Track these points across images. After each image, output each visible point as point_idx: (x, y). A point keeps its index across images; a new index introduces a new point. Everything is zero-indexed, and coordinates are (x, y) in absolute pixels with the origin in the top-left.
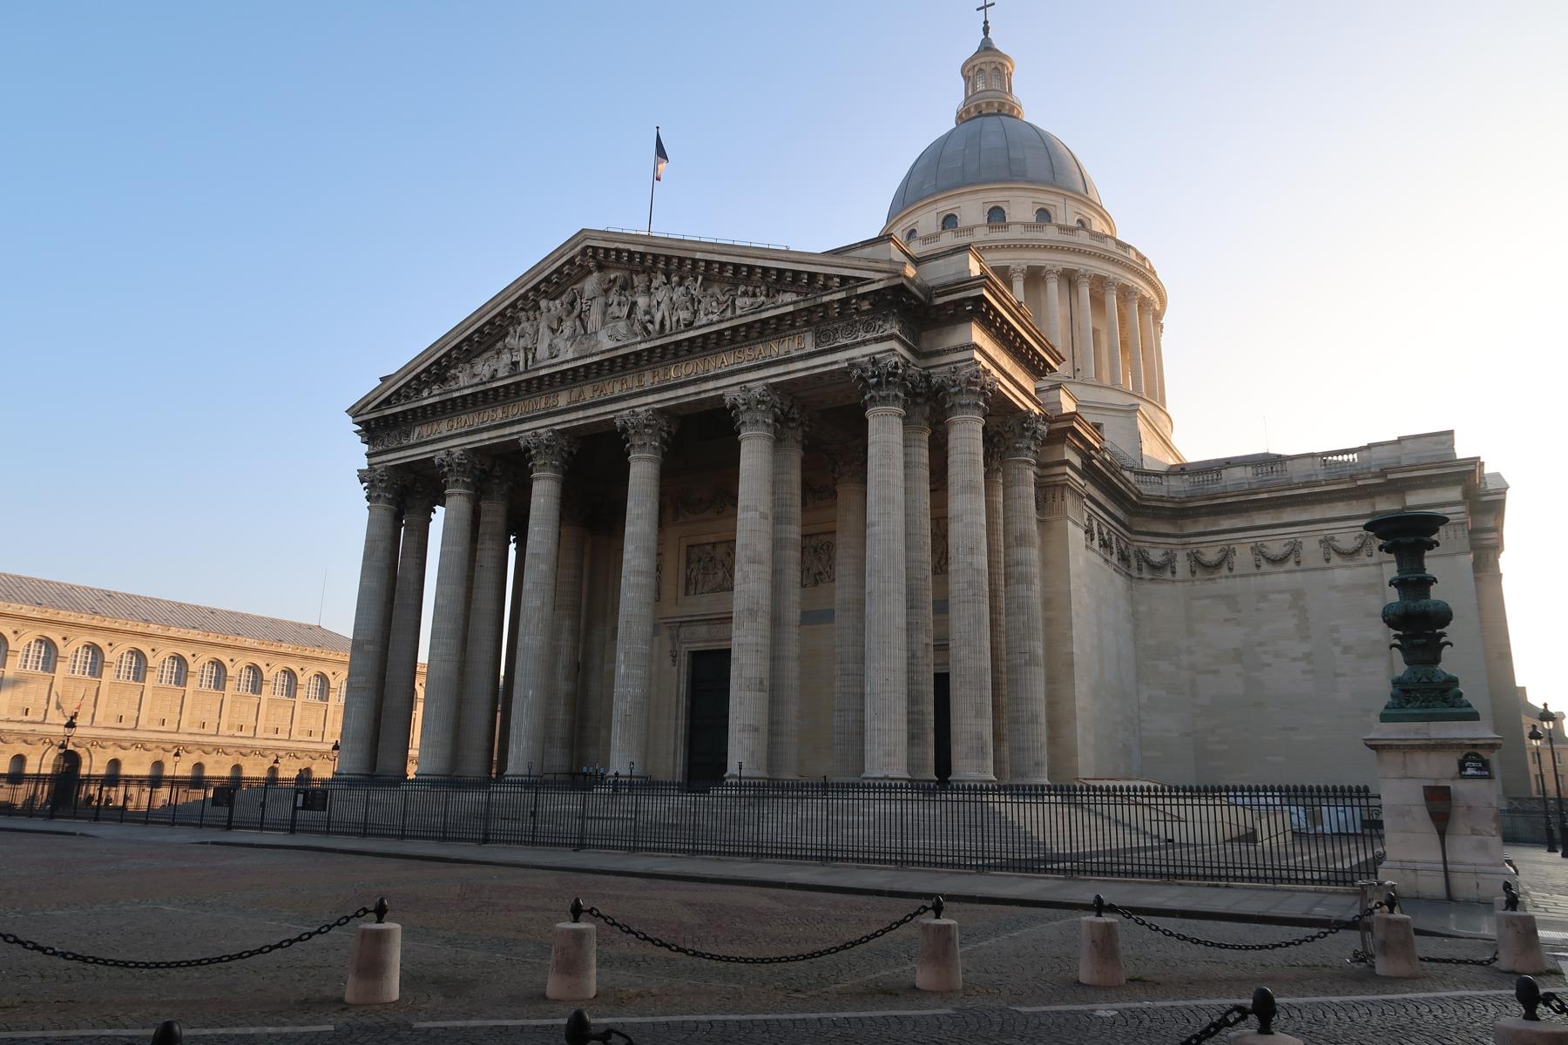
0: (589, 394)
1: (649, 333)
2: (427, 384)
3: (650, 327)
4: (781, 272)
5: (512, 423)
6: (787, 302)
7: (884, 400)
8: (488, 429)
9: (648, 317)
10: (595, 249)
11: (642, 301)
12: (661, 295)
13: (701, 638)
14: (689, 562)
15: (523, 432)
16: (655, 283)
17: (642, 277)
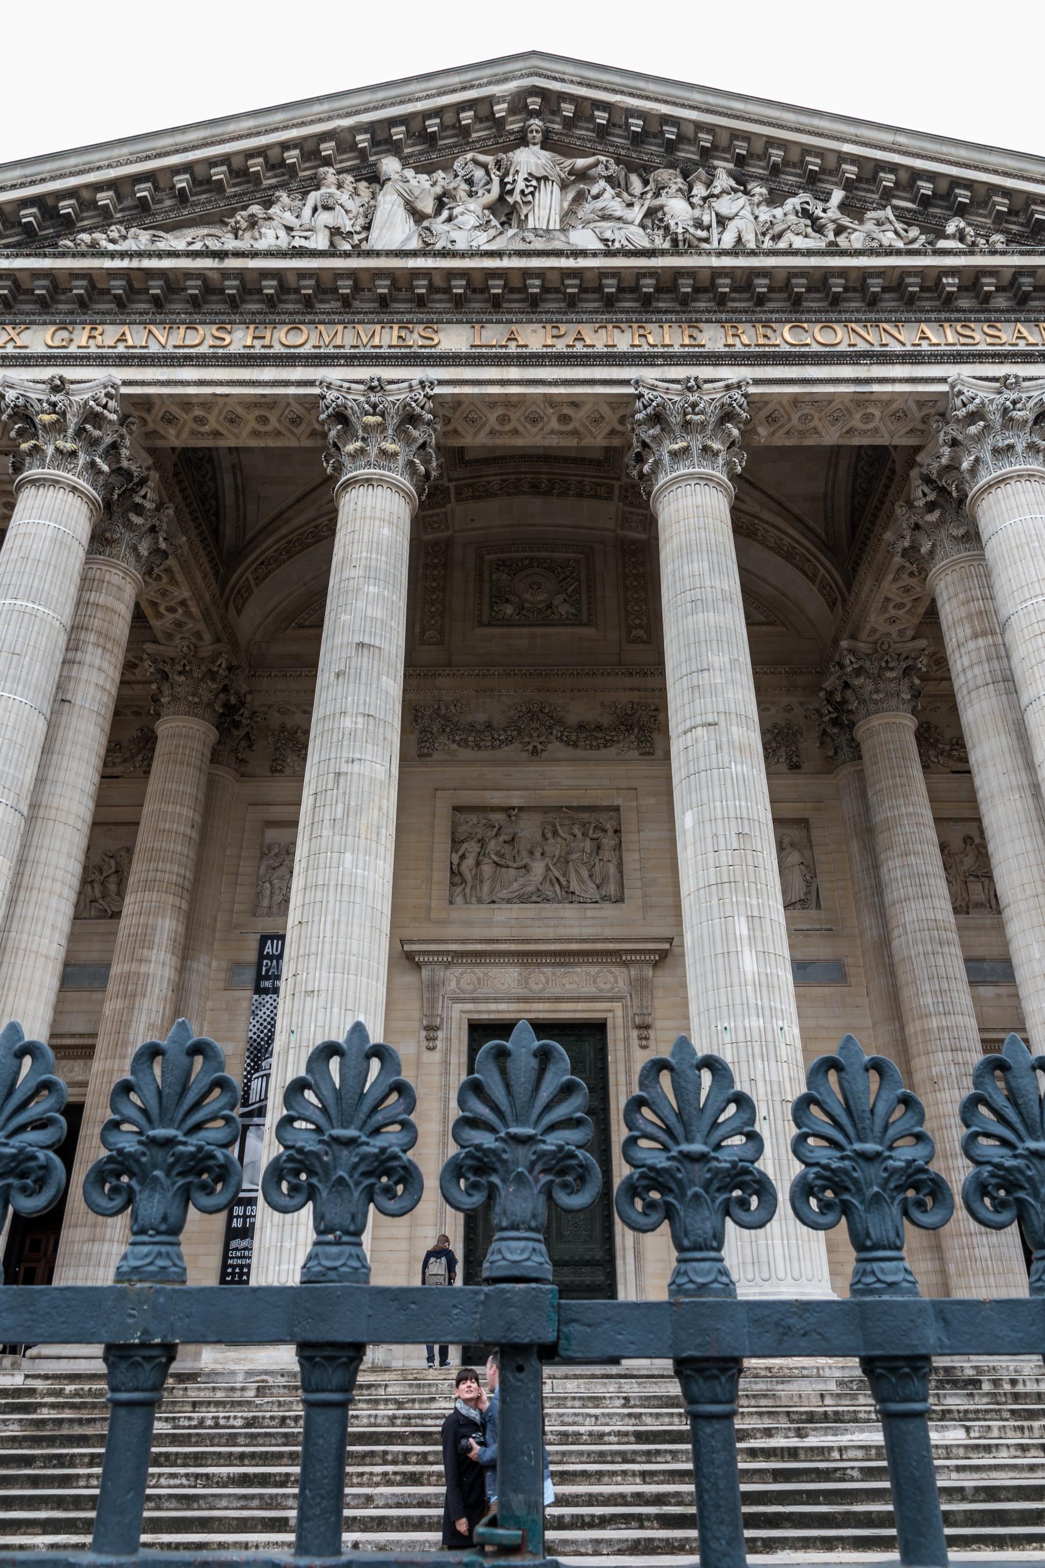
10: (551, 100)
14: (456, 842)
16: (700, 190)
17: (664, 174)
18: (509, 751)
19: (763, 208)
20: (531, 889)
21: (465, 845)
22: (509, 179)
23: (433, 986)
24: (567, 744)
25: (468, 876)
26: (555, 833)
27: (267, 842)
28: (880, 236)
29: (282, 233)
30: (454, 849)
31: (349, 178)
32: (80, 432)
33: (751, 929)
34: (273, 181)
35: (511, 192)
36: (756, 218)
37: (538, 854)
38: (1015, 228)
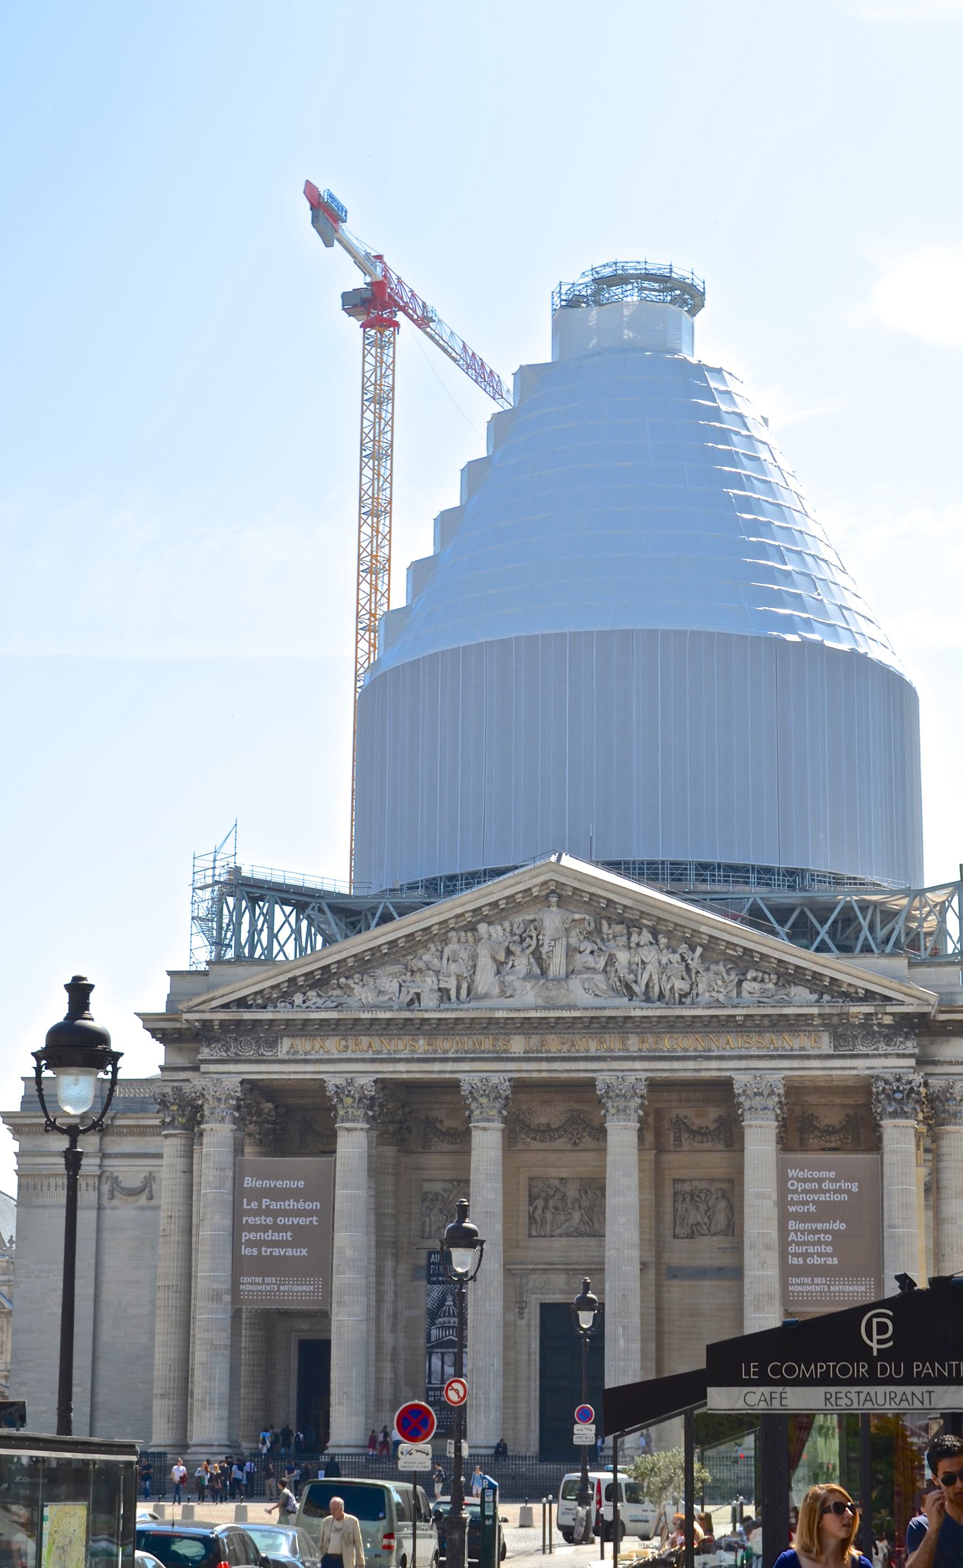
0: (554, 1044)
1: (631, 994)
2: (300, 989)
3: (636, 988)
4: (797, 967)
5: (446, 1060)
6: (801, 1000)
7: (905, 1115)
8: (407, 1060)
9: (632, 976)
11: (623, 957)
12: (650, 955)
13: (559, 1291)
15: (468, 1074)
16: (635, 938)
17: (619, 928)
18: (560, 1143)
19: (665, 951)
20: (572, 1230)
21: (537, 1202)
22: (540, 937)
23: (521, 1286)
24: (594, 1138)
25: (539, 1220)
26: (586, 1193)
27: (425, 1190)
28: (714, 984)
29: (435, 979)
30: (530, 1204)
31: (462, 934)
32: (360, 1100)
33: (624, 1331)
34: (426, 938)
35: (542, 945)
36: (659, 962)
37: (577, 1208)
38: (782, 970)
